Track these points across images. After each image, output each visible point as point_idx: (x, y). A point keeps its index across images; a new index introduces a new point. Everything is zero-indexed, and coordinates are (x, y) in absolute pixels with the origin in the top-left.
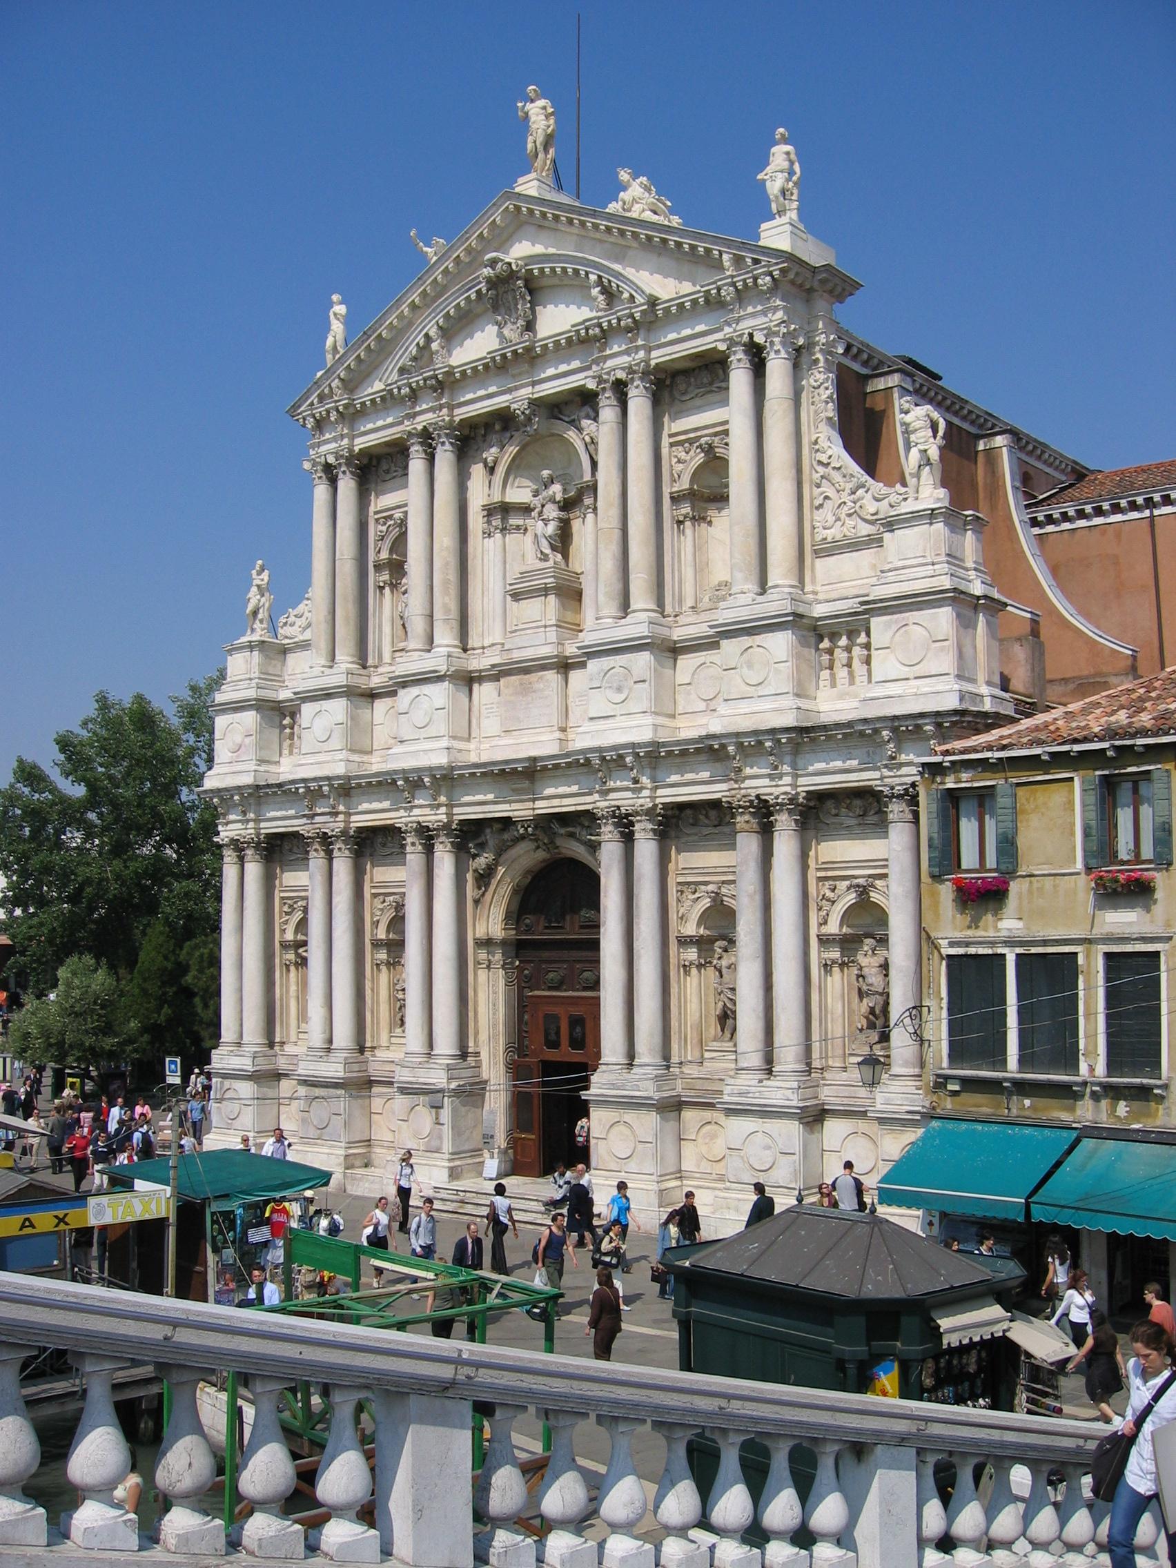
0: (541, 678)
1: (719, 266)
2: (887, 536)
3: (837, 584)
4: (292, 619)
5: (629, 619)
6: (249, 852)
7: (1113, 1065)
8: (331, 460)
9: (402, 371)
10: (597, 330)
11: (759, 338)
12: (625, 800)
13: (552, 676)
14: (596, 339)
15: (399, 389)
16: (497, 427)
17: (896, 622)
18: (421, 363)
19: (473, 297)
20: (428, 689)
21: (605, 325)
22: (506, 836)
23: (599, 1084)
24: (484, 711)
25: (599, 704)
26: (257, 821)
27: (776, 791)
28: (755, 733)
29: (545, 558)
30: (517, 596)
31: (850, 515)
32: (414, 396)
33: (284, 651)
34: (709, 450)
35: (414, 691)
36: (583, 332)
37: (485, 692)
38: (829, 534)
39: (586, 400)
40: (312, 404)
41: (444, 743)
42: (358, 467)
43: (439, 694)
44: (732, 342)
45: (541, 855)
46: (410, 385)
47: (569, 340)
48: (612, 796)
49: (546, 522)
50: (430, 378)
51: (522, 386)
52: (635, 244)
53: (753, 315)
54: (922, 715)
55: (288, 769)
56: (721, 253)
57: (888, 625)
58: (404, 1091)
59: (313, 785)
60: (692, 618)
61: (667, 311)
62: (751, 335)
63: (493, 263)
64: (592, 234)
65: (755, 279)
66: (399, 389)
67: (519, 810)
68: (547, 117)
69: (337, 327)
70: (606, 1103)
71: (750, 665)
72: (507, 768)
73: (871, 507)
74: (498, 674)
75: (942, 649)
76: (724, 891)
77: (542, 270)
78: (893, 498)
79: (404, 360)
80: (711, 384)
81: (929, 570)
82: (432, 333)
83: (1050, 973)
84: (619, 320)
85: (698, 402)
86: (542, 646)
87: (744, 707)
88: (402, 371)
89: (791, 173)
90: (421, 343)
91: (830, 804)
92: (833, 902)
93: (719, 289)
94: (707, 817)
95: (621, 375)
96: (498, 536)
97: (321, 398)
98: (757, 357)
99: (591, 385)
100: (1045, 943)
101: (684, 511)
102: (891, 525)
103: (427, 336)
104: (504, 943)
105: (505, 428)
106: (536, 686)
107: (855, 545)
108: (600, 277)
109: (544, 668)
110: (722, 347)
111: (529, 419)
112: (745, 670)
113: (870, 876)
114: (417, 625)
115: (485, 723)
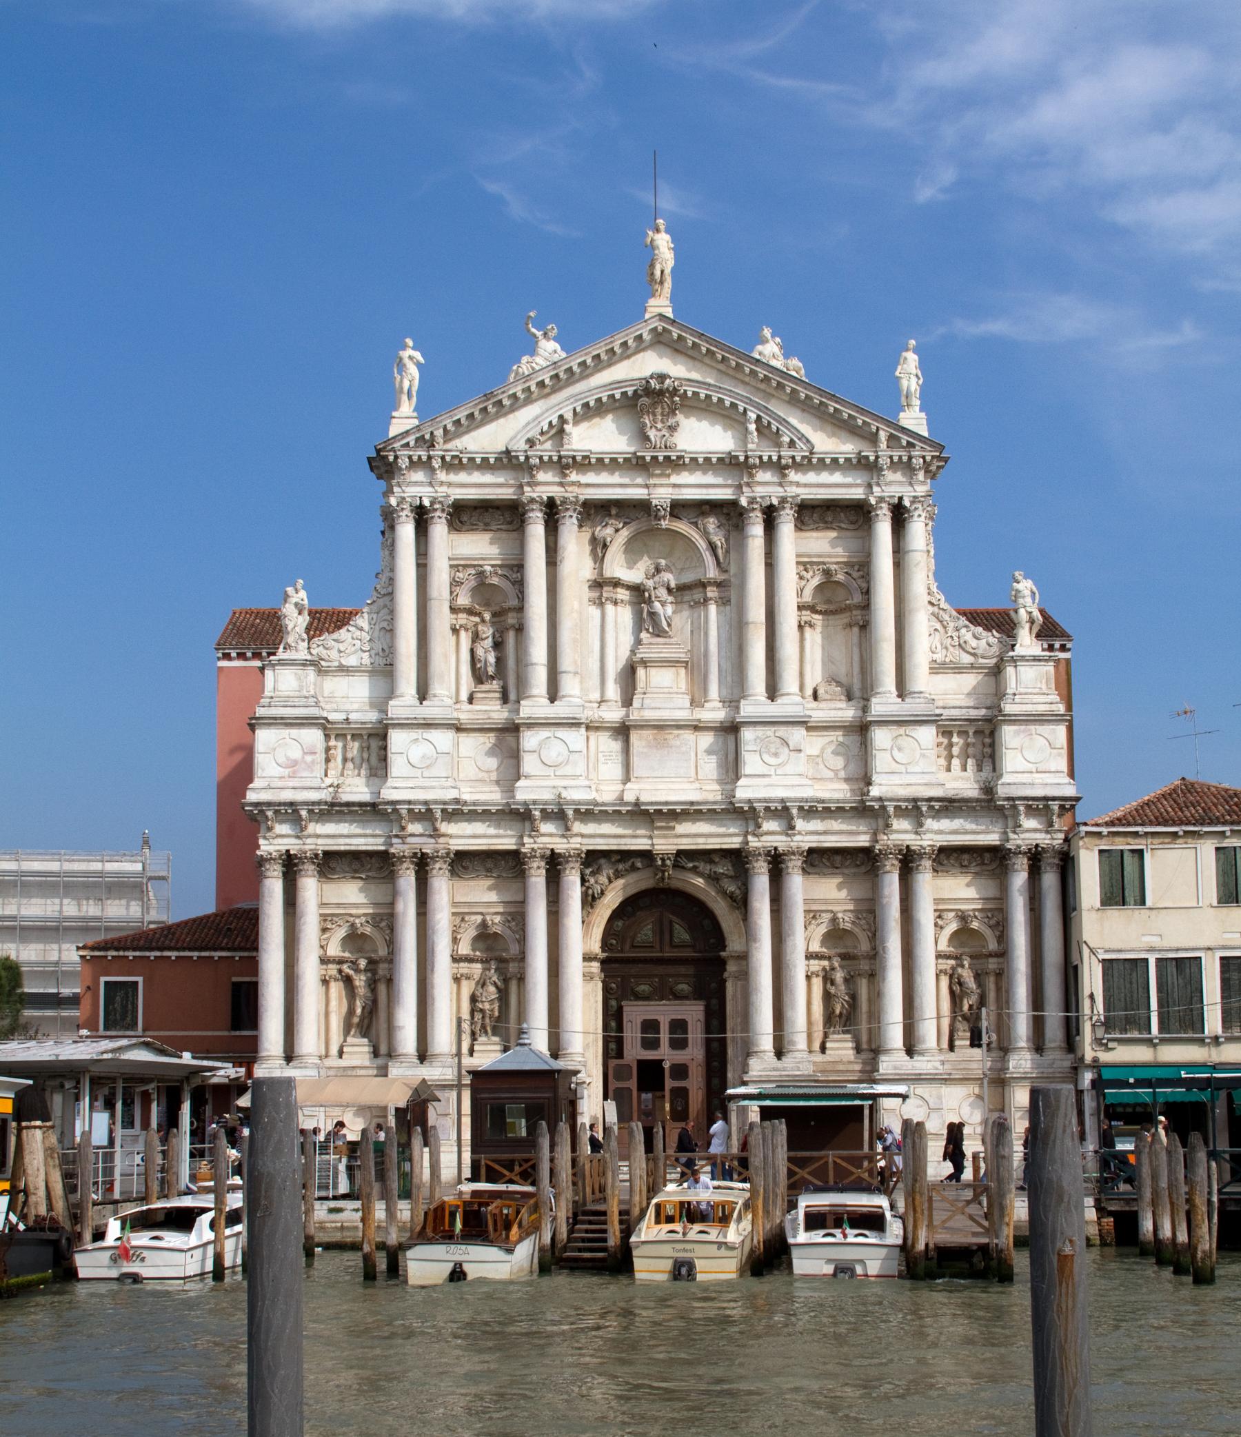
0: (678, 736)
1: (873, 439)
5: (779, 701)
7: (1160, 1032)
8: (426, 503)
9: (531, 442)
10: (757, 461)
11: (907, 503)
15: (527, 458)
17: (1024, 731)
19: (618, 396)
20: (562, 733)
22: (621, 867)
24: (601, 759)
34: (827, 573)
35: (544, 733)
39: (730, 514)
40: (407, 444)
44: (881, 499)
46: (541, 458)
48: (764, 838)
49: (663, 604)
51: (662, 485)
54: (1054, 799)
56: (878, 429)
57: (1017, 733)
59: (417, 808)
61: (821, 460)
62: (901, 498)
64: (747, 379)
65: (910, 458)
69: (413, 371)
71: (900, 749)
72: (665, 808)
79: (534, 433)
82: (569, 416)
84: (780, 457)
87: (896, 779)
88: (531, 442)
90: (554, 423)
92: (942, 928)
94: (829, 859)
95: (775, 502)
96: (609, 607)
97: (420, 440)
98: (900, 515)
99: (744, 502)
103: (561, 417)
105: (618, 516)
106: (673, 742)
108: (759, 417)
109: (679, 727)
112: (895, 752)
115: (602, 768)
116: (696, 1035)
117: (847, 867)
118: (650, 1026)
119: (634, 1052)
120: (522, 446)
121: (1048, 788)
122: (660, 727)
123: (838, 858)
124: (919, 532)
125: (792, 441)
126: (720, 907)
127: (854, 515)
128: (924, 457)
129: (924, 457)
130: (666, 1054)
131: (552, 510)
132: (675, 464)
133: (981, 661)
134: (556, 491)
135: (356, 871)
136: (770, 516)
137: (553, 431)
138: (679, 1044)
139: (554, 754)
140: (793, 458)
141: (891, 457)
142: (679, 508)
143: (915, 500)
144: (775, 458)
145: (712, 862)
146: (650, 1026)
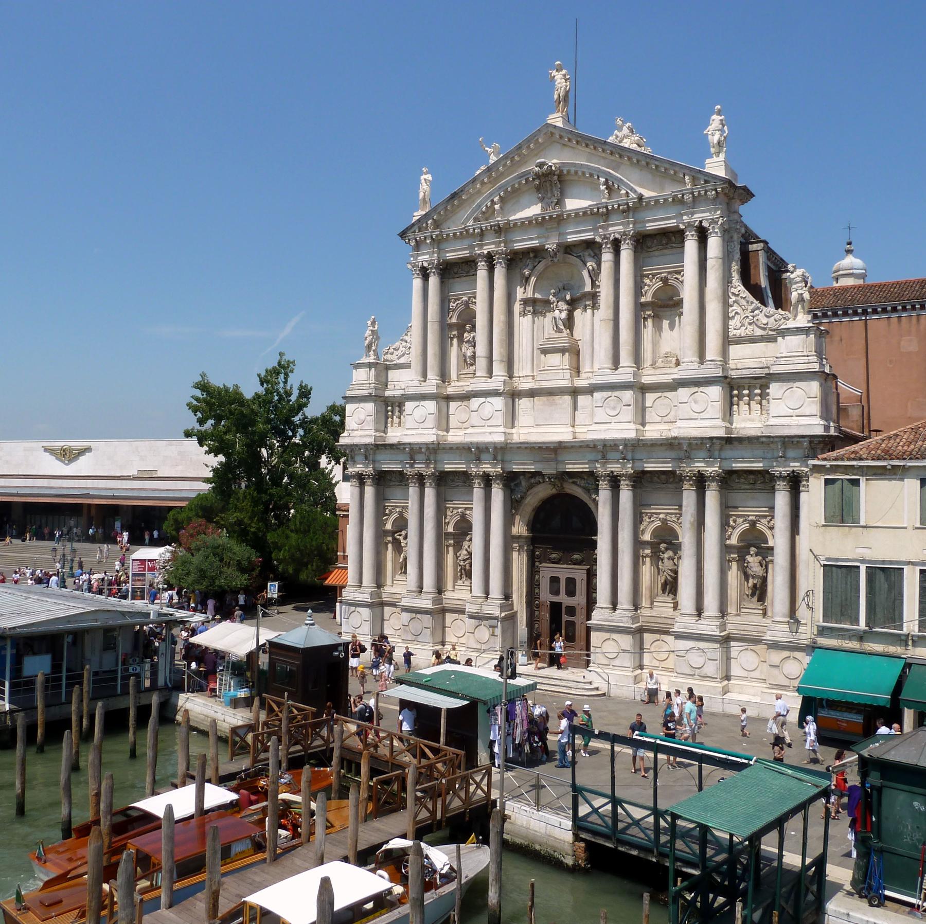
2: (780, 339)
3: (746, 359)
4: (391, 350)
6: (369, 482)
8: (425, 265)
10: (605, 210)
11: (705, 224)
12: (615, 468)
13: (568, 399)
14: (603, 214)
15: (474, 229)
16: (531, 255)
18: (487, 215)
19: (524, 182)
21: (610, 207)
22: (533, 481)
23: (598, 617)
25: (600, 415)
26: (374, 461)
27: (710, 469)
28: (702, 439)
29: (560, 331)
30: (545, 352)
31: (750, 324)
32: (482, 234)
33: (388, 368)
35: (483, 400)
36: (595, 210)
37: (523, 404)
38: (738, 332)
39: (592, 247)
41: (502, 429)
42: (441, 270)
43: (498, 403)
44: (689, 225)
45: (554, 491)
47: (585, 213)
50: (495, 225)
52: (628, 163)
53: (703, 212)
54: (803, 437)
55: (395, 435)
58: (471, 617)
60: (652, 371)
61: (648, 203)
62: (701, 222)
63: (541, 165)
65: (706, 192)
66: (474, 229)
67: (549, 469)
68: (566, 80)
70: (601, 629)
71: (696, 402)
73: (765, 322)
74: (532, 393)
75: (813, 402)
76: (668, 518)
77: (568, 171)
78: (777, 317)
80: (667, 244)
81: (806, 359)
82: (496, 199)
83: (886, 577)
84: (619, 206)
85: (657, 253)
86: (563, 380)
87: (693, 424)
88: (476, 219)
89: (722, 131)
91: (734, 476)
93: (683, 195)
95: (618, 236)
99: (598, 239)
100: (884, 562)
101: (648, 313)
102: (784, 333)
103: (492, 201)
104: (526, 537)
105: (535, 257)
107: (753, 340)
110: (682, 227)
111: (556, 254)
112: (693, 404)
113: (756, 516)
114: (481, 363)
116: (581, 587)
117: (671, 483)
118: (555, 580)
119: (546, 596)
120: (471, 222)
121: (802, 428)
122: (551, 392)
123: (663, 477)
124: (714, 244)
125: (627, 193)
126: (592, 506)
127: (671, 239)
128: (716, 190)
129: (716, 190)
130: (563, 598)
131: (490, 259)
132: (560, 221)
133: (771, 333)
134: (492, 248)
135: (401, 481)
136: (616, 245)
137: (490, 211)
138: (571, 592)
139: (486, 413)
140: (627, 204)
141: (692, 193)
142: (568, 249)
143: (713, 222)
144: (616, 206)
145: (582, 478)
146: (555, 580)
